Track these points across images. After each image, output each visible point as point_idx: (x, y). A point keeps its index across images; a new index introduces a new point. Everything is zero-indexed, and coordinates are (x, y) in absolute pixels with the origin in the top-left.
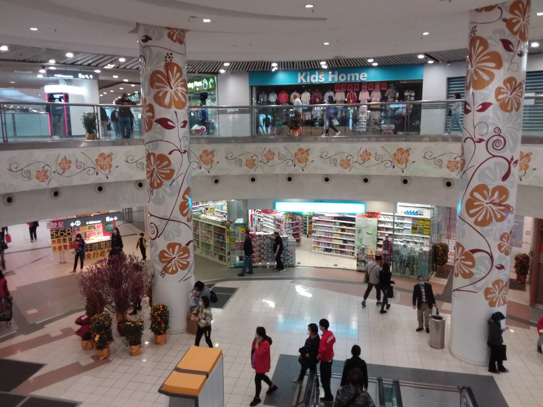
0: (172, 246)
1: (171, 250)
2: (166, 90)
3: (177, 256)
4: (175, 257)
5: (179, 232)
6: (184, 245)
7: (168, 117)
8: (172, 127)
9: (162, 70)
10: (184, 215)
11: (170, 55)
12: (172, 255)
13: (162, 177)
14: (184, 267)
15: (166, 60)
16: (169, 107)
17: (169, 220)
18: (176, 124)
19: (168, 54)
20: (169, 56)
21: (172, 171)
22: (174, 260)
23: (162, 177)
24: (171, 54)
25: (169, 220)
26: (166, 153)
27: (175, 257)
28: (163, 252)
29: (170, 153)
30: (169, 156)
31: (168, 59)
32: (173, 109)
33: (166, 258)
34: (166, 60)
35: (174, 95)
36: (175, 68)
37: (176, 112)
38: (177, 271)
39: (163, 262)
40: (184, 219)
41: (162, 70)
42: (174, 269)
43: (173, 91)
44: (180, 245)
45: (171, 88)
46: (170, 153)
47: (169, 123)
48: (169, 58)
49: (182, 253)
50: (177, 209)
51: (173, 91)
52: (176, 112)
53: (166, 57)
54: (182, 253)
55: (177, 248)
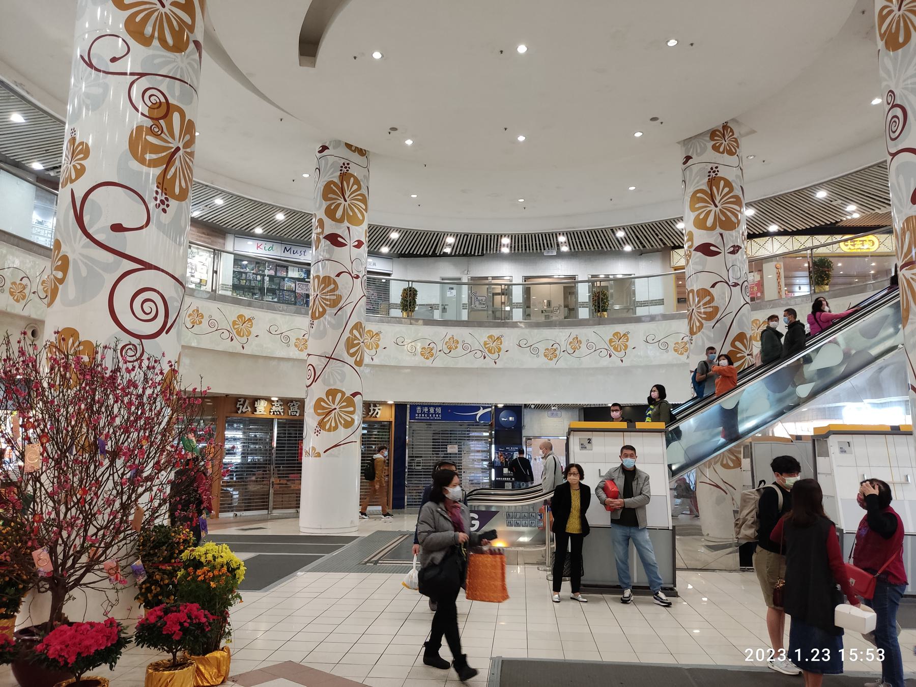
0: (332, 393)
1: (330, 398)
2: (339, 202)
3: (337, 407)
4: (335, 409)
5: (343, 375)
6: (348, 394)
7: (339, 232)
8: (342, 245)
9: (336, 180)
10: (352, 355)
11: (346, 165)
12: (332, 404)
13: (325, 304)
14: (348, 425)
15: (341, 170)
16: (341, 221)
17: (330, 358)
18: (348, 241)
19: (344, 164)
20: (346, 166)
21: (340, 298)
22: (334, 412)
23: (325, 304)
24: (348, 164)
25: (330, 358)
26: (333, 276)
27: (335, 409)
28: (320, 400)
29: (338, 275)
30: (337, 279)
31: (343, 169)
32: (346, 224)
33: (324, 408)
34: (341, 170)
35: (349, 209)
36: (352, 180)
37: (348, 228)
38: (336, 428)
39: (319, 414)
40: (351, 361)
41: (336, 180)
42: (333, 424)
43: (346, 204)
44: (343, 394)
45: (346, 201)
46: (338, 275)
47: (339, 239)
48: (346, 168)
49: (344, 404)
50: (342, 345)
51: (346, 204)
52: (348, 228)
53: (342, 167)
54: (344, 404)
55: (339, 396)
